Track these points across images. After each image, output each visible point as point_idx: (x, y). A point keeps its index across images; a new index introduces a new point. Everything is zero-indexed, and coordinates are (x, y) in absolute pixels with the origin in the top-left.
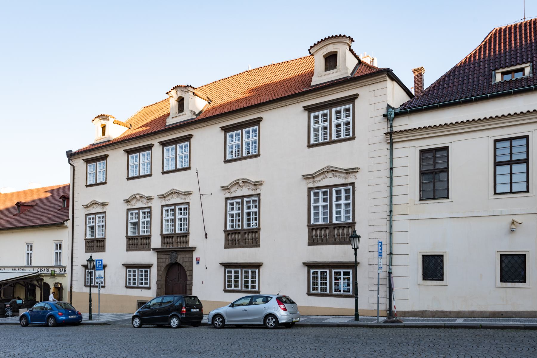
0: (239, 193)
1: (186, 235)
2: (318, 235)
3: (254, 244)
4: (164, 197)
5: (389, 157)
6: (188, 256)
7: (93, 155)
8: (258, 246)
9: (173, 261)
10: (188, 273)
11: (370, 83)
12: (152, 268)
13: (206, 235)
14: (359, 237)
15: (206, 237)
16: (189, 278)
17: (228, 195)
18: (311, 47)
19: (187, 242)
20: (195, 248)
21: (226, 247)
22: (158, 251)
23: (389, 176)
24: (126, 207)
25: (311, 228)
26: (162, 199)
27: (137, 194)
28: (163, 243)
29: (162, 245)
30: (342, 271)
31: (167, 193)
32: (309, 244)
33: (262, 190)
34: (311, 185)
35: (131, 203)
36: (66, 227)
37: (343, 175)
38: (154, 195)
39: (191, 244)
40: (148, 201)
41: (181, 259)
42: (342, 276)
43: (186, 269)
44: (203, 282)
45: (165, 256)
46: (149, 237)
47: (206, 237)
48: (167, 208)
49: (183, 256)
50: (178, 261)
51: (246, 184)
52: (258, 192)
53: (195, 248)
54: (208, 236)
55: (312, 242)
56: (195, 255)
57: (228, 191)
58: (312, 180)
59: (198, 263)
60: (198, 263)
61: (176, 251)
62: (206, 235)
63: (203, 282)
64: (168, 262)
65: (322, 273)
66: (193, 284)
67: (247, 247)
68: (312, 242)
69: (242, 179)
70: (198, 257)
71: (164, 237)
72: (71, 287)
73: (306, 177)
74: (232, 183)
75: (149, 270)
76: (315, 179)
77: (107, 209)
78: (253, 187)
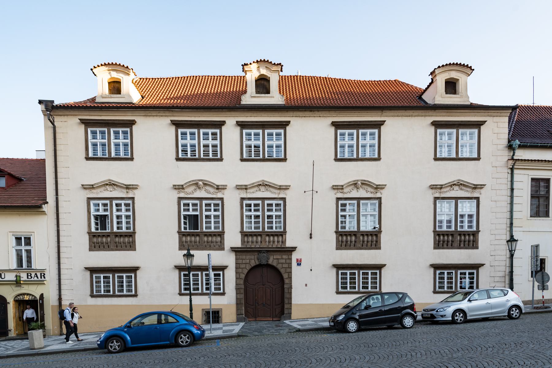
0: (355, 194)
1: (282, 234)
2: (443, 239)
3: (373, 246)
4: (246, 189)
5: (509, 179)
6: (284, 257)
7: (105, 119)
8: (380, 248)
9: (264, 262)
10: (285, 276)
11: (495, 114)
12: (226, 271)
13: (311, 234)
14: (516, 241)
15: (311, 238)
16: (286, 281)
17: (340, 195)
18: (439, 67)
19: (284, 242)
20: (296, 248)
21: (337, 249)
22: (235, 250)
23: (509, 194)
24: (175, 195)
25: (437, 234)
26: (240, 191)
27: (200, 180)
28: (243, 242)
29: (242, 244)
30: (467, 272)
31: (253, 184)
32: (435, 248)
33: (384, 194)
34: (437, 195)
35: (186, 190)
36: (44, 213)
37: (468, 189)
38: (231, 184)
39: (289, 244)
40: (216, 191)
41: (275, 260)
42: (467, 276)
43: (282, 271)
44: (306, 285)
45: (248, 257)
46: (221, 234)
47: (311, 238)
48: (249, 202)
49: (279, 257)
50: (270, 262)
51: (365, 187)
52: (378, 195)
53: (296, 248)
54: (313, 236)
55: (438, 245)
56: (295, 256)
57: (341, 191)
58: (439, 190)
59: (299, 264)
60: (299, 264)
61: (268, 251)
62: (311, 234)
63: (306, 285)
64: (253, 263)
65: (448, 273)
66: (293, 287)
67: (365, 249)
68: (438, 245)
69: (362, 180)
70: (299, 258)
71: (244, 234)
72: (60, 299)
73: (433, 187)
74: (349, 183)
75: (221, 273)
76: (442, 190)
77: (136, 194)
78: (372, 190)
